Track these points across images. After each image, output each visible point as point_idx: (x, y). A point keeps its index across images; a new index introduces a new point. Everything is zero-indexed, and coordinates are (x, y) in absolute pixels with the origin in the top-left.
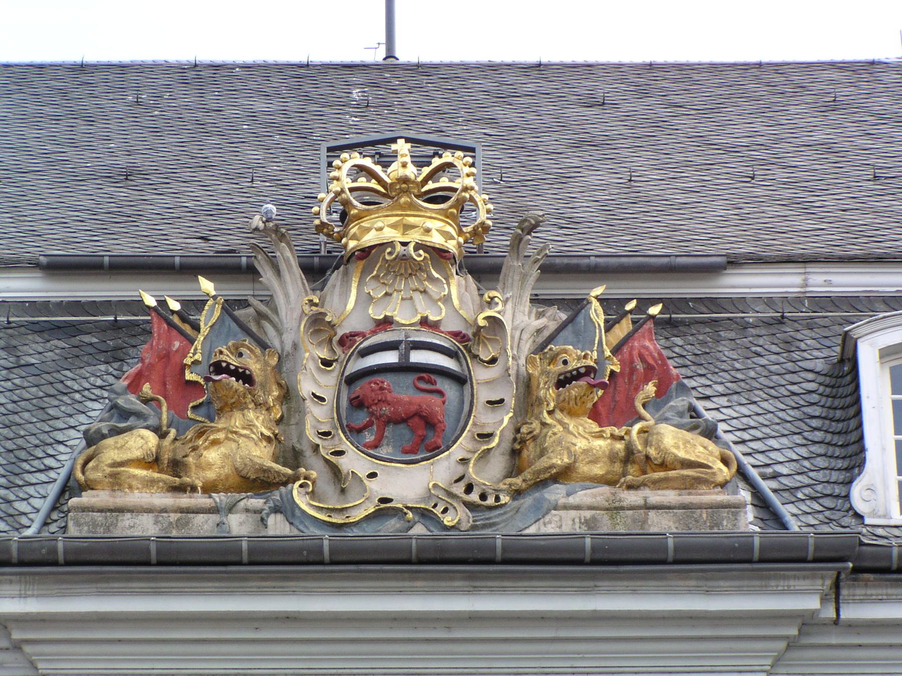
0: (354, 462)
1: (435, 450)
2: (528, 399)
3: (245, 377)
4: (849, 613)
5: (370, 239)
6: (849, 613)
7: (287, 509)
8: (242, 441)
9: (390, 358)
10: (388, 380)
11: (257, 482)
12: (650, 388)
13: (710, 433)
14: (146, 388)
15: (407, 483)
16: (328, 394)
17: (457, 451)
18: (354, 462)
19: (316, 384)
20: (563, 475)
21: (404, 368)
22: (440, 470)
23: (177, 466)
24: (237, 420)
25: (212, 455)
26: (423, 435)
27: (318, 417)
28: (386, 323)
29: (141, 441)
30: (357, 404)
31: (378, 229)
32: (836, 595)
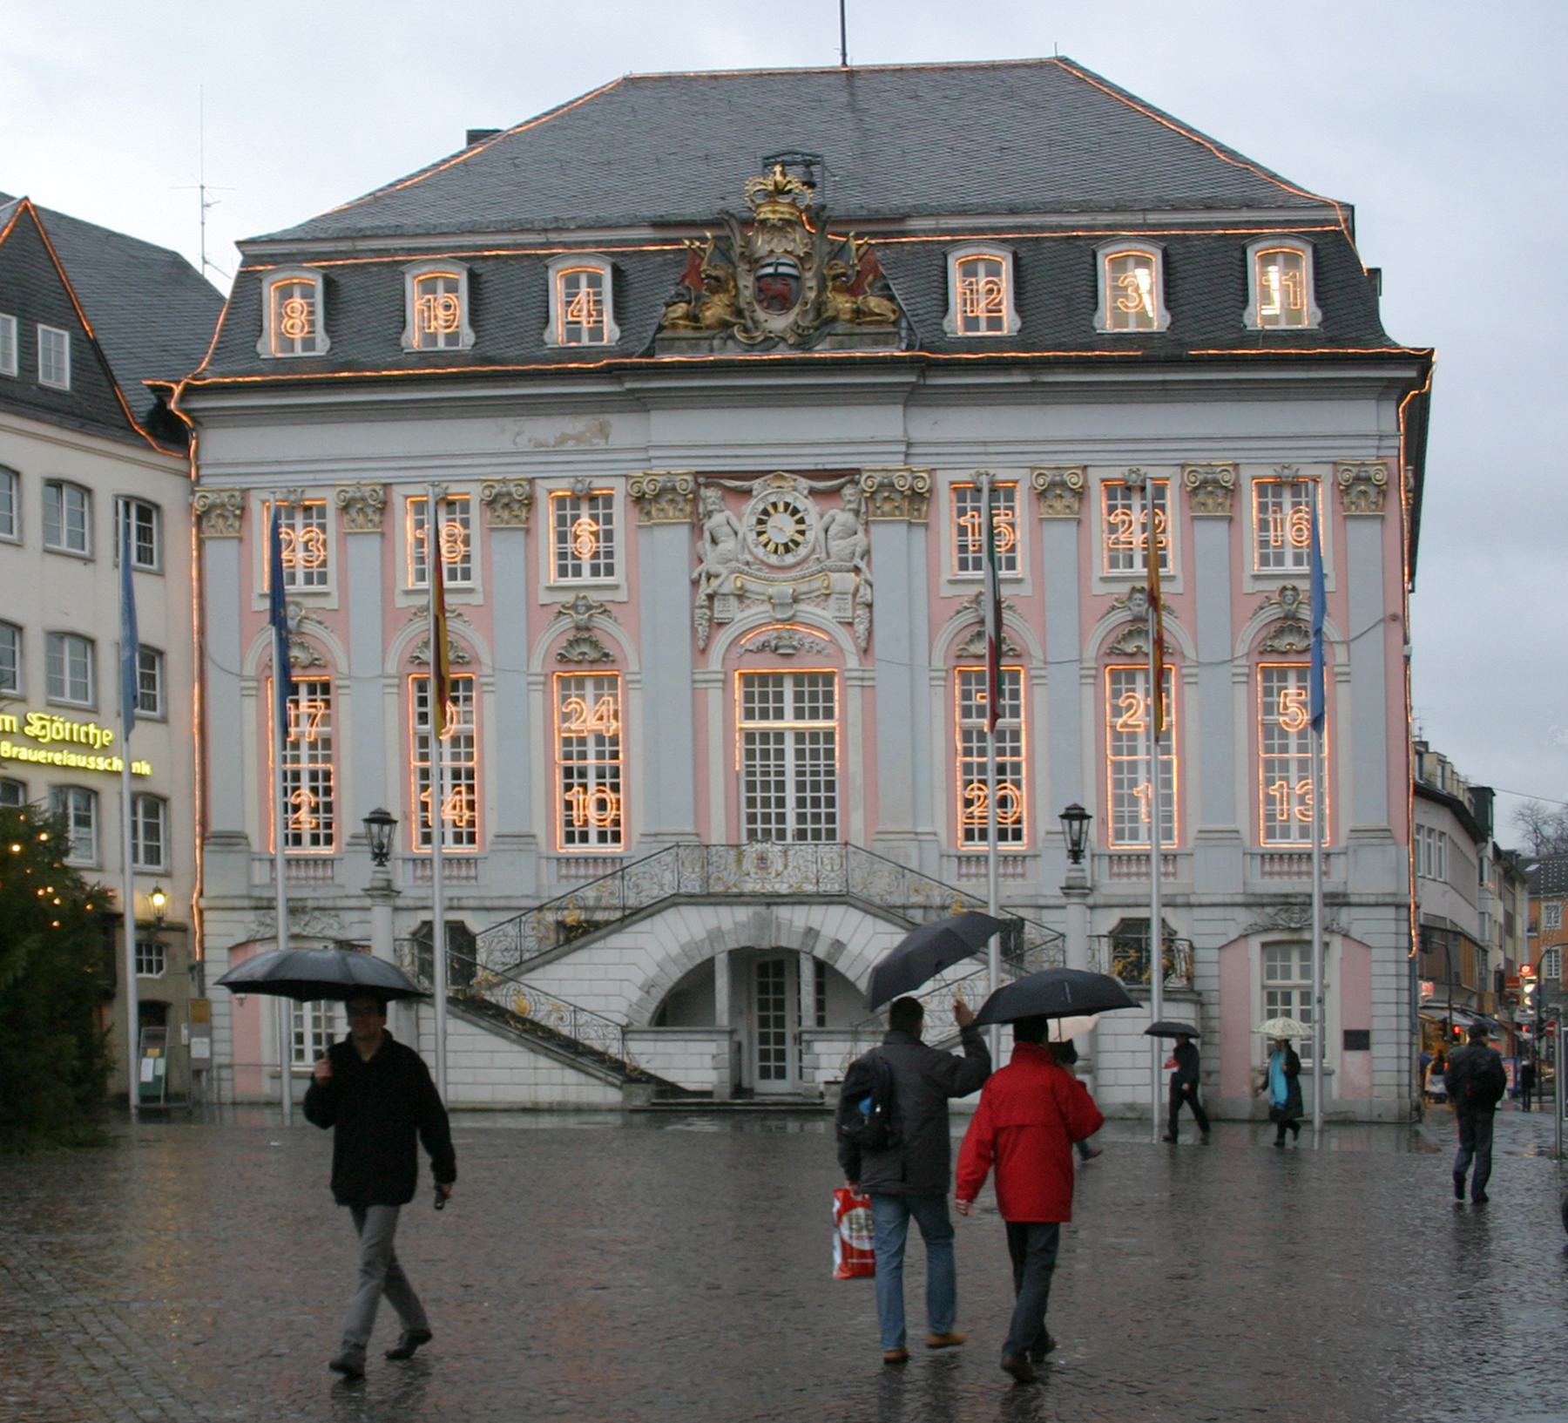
0: (761, 315)
1: (789, 309)
2: (822, 289)
3: (717, 279)
4: (931, 381)
5: (762, 216)
6: (931, 381)
7: (732, 337)
9: (770, 270)
10: (769, 280)
11: (725, 325)
12: (870, 278)
13: (892, 298)
14: (687, 283)
15: (778, 323)
16: (750, 284)
17: (797, 309)
18: (761, 315)
19: (746, 283)
20: (834, 319)
21: (775, 275)
22: (791, 316)
23: (695, 319)
24: (716, 298)
25: (708, 314)
28: (772, 251)
29: (681, 308)
30: (760, 290)
31: (766, 213)
32: (924, 377)
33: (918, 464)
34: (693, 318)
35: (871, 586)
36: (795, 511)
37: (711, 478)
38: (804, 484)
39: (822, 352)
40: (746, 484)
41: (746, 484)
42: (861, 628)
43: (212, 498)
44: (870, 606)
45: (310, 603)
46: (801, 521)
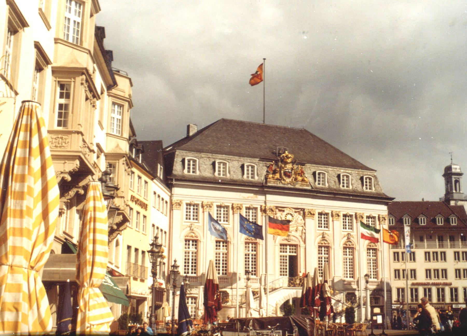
8: (278, 176)
11: (279, 180)
15: (288, 180)
17: (292, 178)
26: (289, 177)
27: (283, 174)
33: (314, 208)
34: (273, 177)
35: (305, 230)
36: (291, 215)
37: (277, 207)
38: (294, 210)
39: (298, 186)
40: (283, 209)
41: (283, 209)
42: (303, 237)
43: (176, 201)
44: (305, 233)
45: (195, 224)
46: (293, 217)
